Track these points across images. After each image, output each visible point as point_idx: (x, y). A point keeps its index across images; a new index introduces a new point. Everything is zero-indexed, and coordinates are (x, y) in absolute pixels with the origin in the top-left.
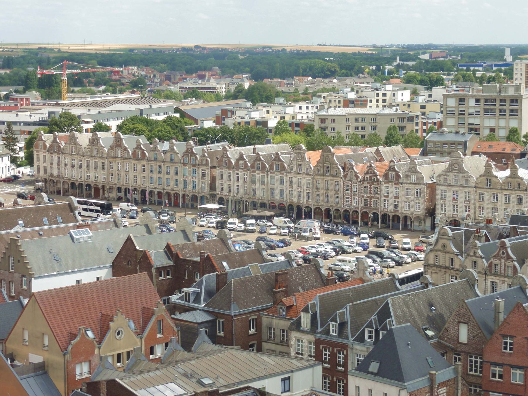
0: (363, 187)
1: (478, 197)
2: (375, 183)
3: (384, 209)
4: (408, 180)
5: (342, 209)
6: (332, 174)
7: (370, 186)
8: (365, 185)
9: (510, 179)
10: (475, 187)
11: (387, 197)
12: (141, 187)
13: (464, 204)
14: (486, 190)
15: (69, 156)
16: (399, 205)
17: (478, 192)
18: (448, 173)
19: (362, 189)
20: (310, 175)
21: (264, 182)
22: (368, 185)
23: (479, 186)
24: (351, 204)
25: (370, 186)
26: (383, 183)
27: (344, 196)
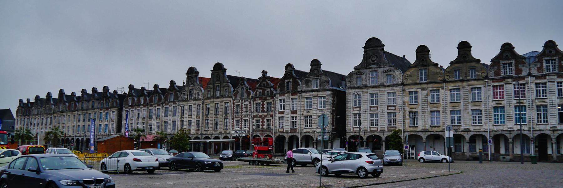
0: (255, 105)
1: (407, 99)
2: (269, 98)
3: (278, 129)
4: (308, 87)
5: (231, 135)
6: (222, 94)
7: (263, 102)
8: (257, 102)
9: (457, 65)
10: (403, 84)
11: (283, 113)
12: (71, 136)
13: (386, 111)
14: (419, 86)
15: (33, 117)
16: (298, 121)
17: (407, 91)
18: (362, 71)
19: (253, 107)
20: (200, 100)
21: (159, 116)
22: (260, 101)
23: (409, 81)
24: (241, 128)
25: (263, 102)
26: (277, 96)
27: (233, 119)
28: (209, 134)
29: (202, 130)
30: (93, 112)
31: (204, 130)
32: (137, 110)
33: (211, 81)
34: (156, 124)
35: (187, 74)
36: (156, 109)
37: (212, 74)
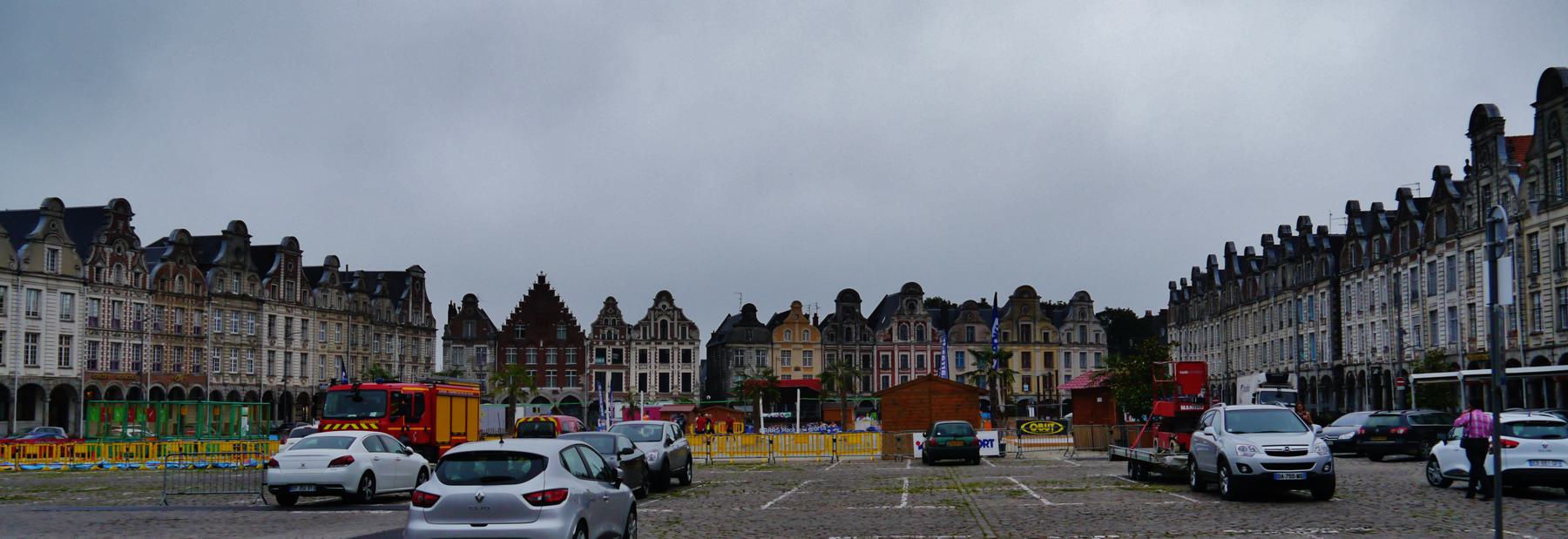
28: (1544, 348)
29: (1524, 334)
30: (1286, 299)
31: (1529, 333)
32: (1368, 282)
33: (1537, 147)
34: (1411, 322)
35: (1472, 133)
36: (1409, 271)
37: (1537, 118)
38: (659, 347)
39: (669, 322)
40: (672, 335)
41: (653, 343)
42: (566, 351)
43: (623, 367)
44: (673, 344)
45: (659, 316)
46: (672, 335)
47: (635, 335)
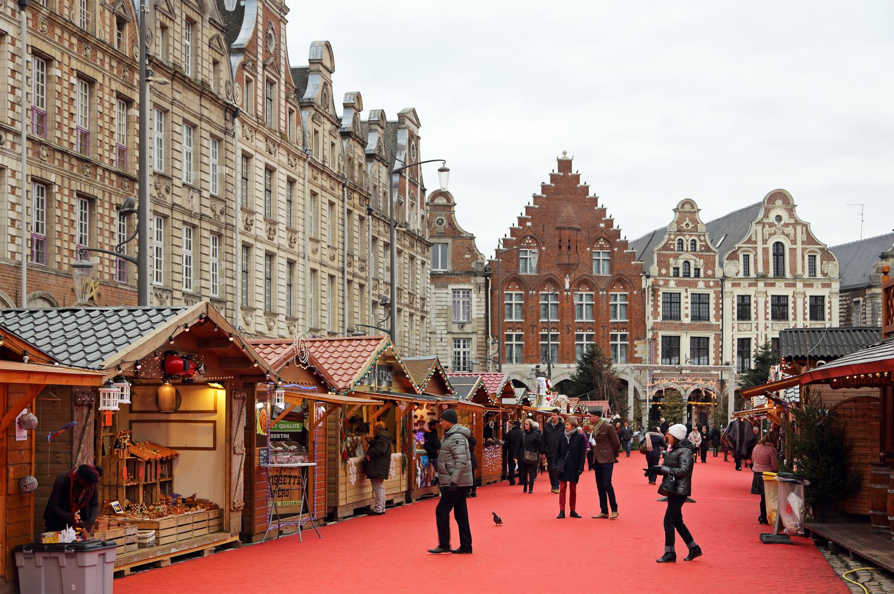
38: (773, 291)
39: (788, 245)
40: (793, 270)
41: (761, 284)
42: (608, 297)
43: (709, 327)
44: (794, 285)
45: (771, 235)
46: (793, 270)
47: (734, 268)
